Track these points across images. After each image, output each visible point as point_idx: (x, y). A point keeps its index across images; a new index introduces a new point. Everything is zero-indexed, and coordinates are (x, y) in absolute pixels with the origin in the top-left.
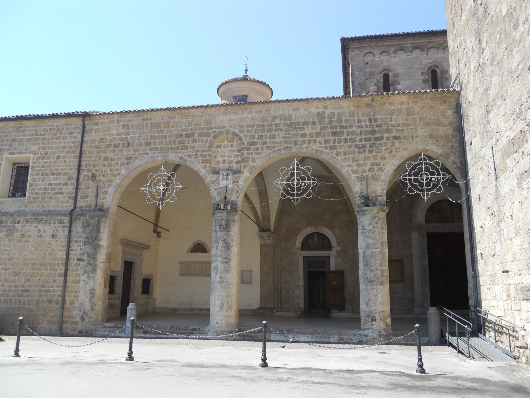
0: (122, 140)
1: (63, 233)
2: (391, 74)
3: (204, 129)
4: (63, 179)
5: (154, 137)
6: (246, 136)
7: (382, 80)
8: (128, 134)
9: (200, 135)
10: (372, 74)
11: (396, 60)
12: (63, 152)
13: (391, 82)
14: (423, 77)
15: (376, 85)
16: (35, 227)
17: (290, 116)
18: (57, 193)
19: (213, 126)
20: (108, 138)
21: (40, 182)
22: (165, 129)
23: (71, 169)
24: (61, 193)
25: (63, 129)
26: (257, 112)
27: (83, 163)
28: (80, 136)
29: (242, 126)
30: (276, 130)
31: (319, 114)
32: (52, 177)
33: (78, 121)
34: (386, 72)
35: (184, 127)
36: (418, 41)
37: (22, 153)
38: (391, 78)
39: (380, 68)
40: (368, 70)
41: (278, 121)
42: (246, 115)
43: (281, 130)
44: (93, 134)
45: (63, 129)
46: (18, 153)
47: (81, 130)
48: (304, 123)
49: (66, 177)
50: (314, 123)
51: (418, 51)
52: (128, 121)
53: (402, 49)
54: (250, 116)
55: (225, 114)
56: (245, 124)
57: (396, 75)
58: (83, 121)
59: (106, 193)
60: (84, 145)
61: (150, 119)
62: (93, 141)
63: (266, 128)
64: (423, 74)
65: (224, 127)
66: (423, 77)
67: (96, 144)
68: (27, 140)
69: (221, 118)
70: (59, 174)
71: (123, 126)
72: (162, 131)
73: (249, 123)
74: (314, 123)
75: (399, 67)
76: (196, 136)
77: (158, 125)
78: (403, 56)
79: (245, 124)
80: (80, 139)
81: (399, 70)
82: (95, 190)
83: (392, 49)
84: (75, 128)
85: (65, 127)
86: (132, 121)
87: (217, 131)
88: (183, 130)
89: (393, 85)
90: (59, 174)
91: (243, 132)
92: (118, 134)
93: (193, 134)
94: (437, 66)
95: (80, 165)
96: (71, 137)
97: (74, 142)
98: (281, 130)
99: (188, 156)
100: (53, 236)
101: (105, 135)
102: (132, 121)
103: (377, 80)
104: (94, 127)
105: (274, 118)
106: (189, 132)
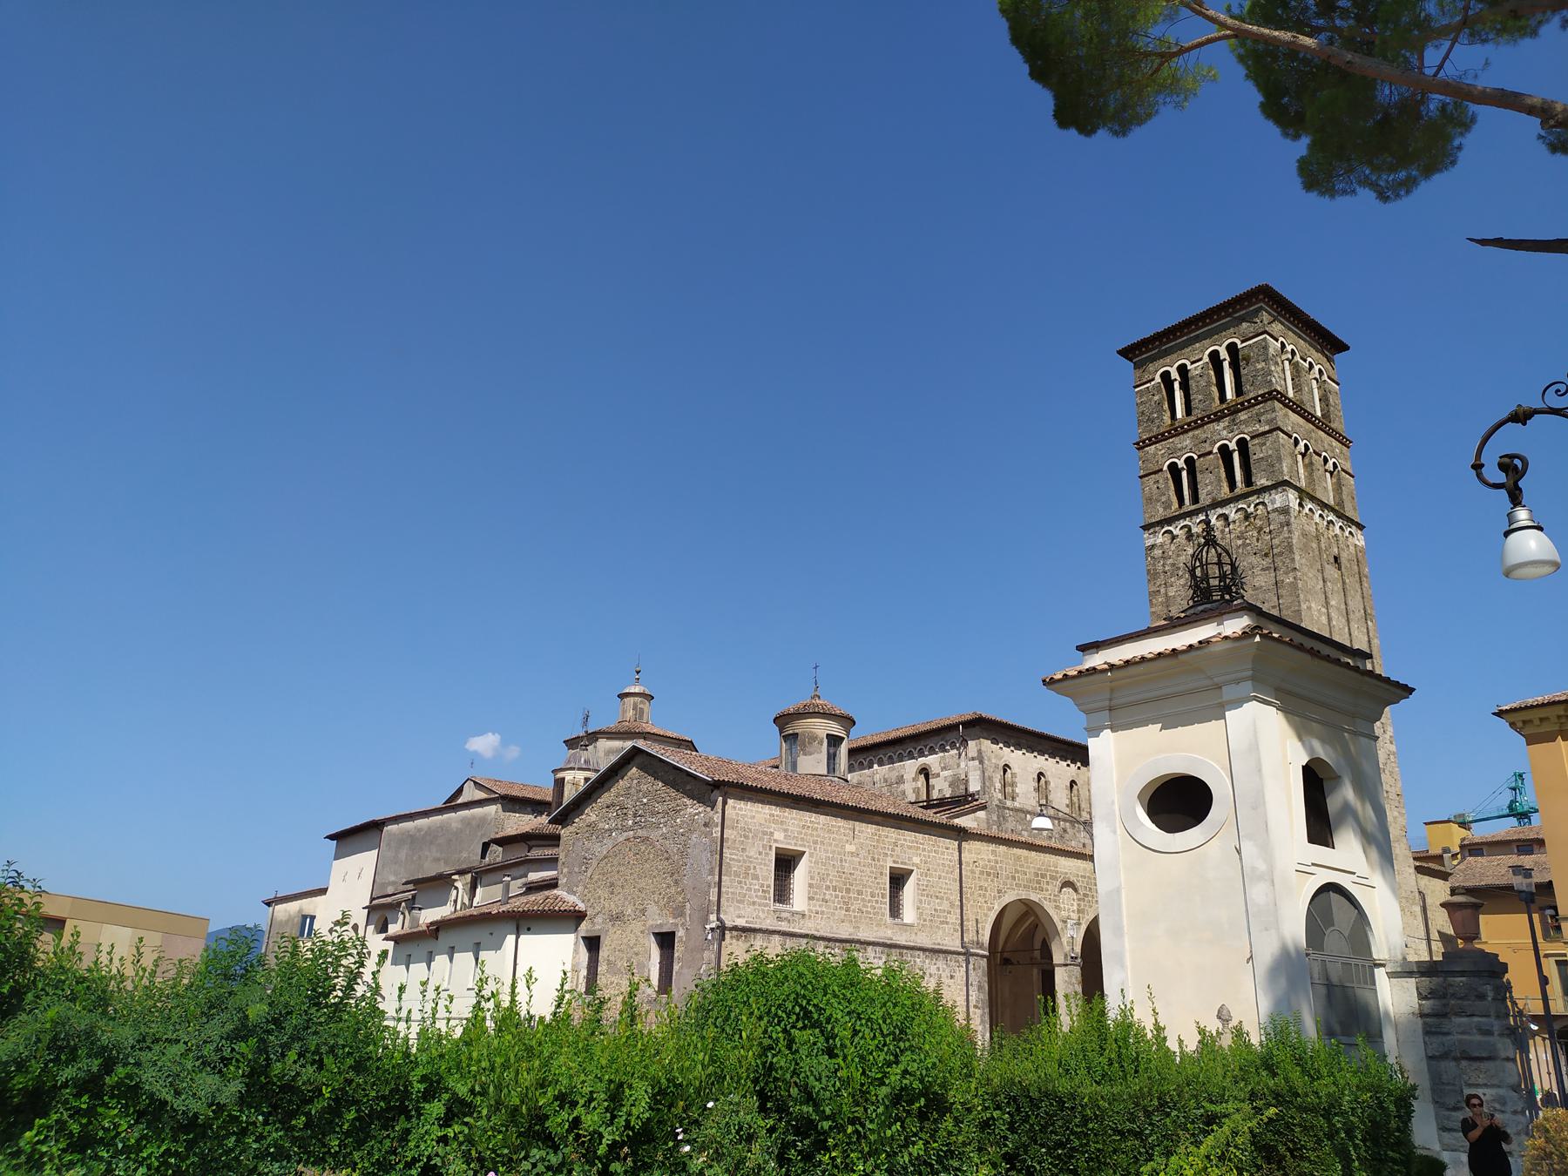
0: (992, 868)
1: (960, 974)
4: (945, 905)
6: (1081, 886)
9: (1052, 878)
16: (935, 964)
18: (942, 923)
21: (926, 906)
24: (947, 923)
32: (937, 901)
37: (905, 864)
46: (902, 863)
59: (983, 929)
68: (910, 847)
81: (1015, 768)
82: (974, 923)
90: (942, 898)
99: (1045, 898)
100: (952, 977)
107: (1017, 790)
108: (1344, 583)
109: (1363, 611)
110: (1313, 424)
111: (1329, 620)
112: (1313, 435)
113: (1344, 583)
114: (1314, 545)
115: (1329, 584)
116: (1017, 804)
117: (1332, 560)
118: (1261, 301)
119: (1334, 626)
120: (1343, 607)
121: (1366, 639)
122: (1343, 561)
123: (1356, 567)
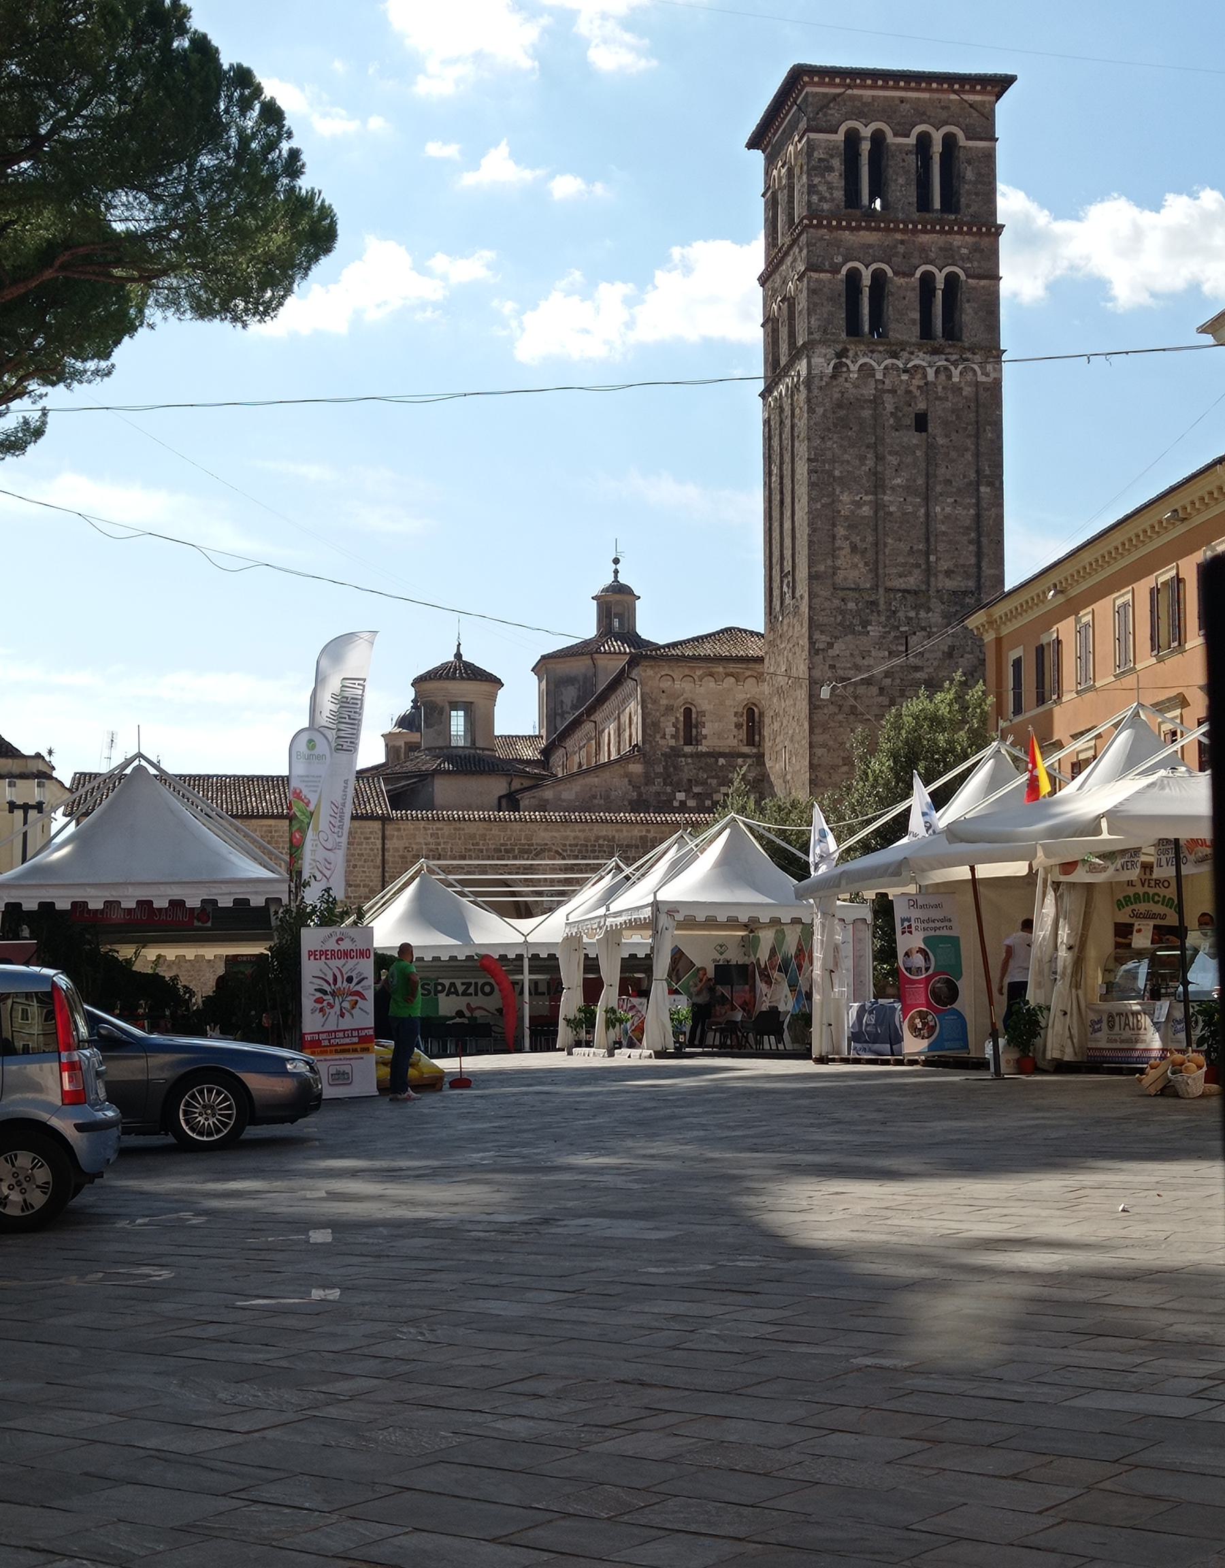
0: (431, 850)
2: (694, 710)
3: (524, 845)
5: (470, 850)
7: (682, 719)
8: (439, 844)
10: (670, 709)
11: (702, 690)
12: (360, 860)
13: (694, 721)
14: (735, 719)
15: (674, 726)
17: (614, 837)
19: (534, 842)
20: (414, 846)
22: (481, 842)
23: (372, 881)
25: (356, 833)
26: (580, 831)
27: (386, 874)
28: (379, 843)
29: (565, 845)
30: (599, 852)
31: (641, 837)
33: (377, 825)
34: (688, 706)
35: (502, 841)
36: (732, 667)
38: (694, 716)
39: (681, 700)
40: (664, 702)
41: (601, 842)
42: (568, 833)
43: (605, 852)
44: (395, 840)
45: (356, 833)
47: (380, 835)
48: (627, 846)
49: (367, 890)
50: (637, 847)
51: (732, 680)
52: (437, 829)
53: (711, 675)
54: (573, 834)
55: (546, 830)
56: (568, 843)
57: (703, 713)
58: (383, 826)
60: (386, 854)
61: (463, 829)
62: (397, 850)
63: (590, 848)
64: (736, 714)
65: (546, 844)
66: (735, 719)
67: (401, 853)
69: (543, 834)
70: (359, 886)
71: (432, 835)
72: (477, 844)
73: (573, 842)
74: (637, 847)
75: (706, 701)
76: (516, 851)
77: (472, 837)
78: (710, 684)
79: (568, 843)
80: (380, 846)
81: (705, 706)
83: (699, 672)
84: (371, 833)
85: (359, 831)
86: (442, 829)
87: (539, 848)
88: (502, 845)
89: (696, 727)
90: (359, 886)
91: (566, 851)
92: (426, 844)
93: (514, 850)
94: (756, 706)
95: (383, 876)
96: (367, 844)
97: (372, 850)
98: (605, 852)
101: (410, 843)
102: (442, 829)
103: (677, 718)
104: (396, 833)
105: (598, 838)
106: (509, 847)
107: (704, 732)
108: (931, 447)
109: (973, 476)
110: (905, 231)
111: (878, 506)
112: (901, 249)
113: (931, 447)
114: (867, 413)
115: (893, 460)
116: (702, 748)
117: (909, 421)
118: (806, 84)
119: (891, 514)
120: (920, 481)
121: (972, 511)
122: (938, 412)
123: (972, 416)
